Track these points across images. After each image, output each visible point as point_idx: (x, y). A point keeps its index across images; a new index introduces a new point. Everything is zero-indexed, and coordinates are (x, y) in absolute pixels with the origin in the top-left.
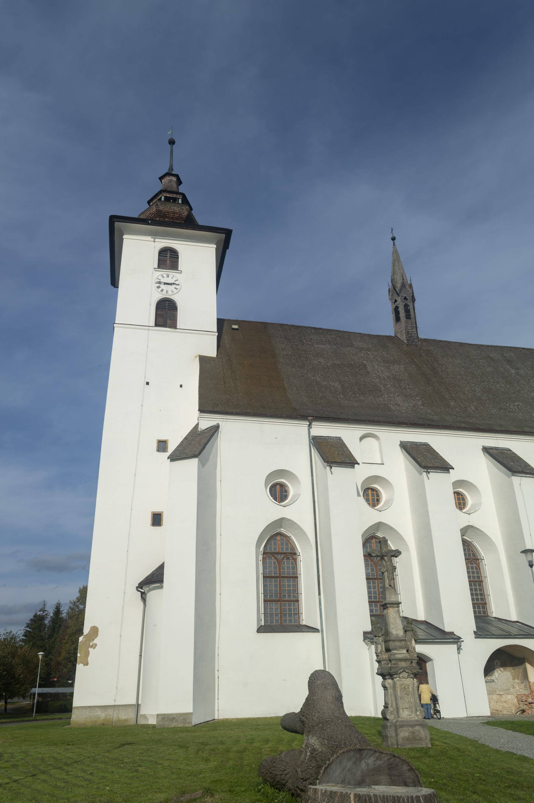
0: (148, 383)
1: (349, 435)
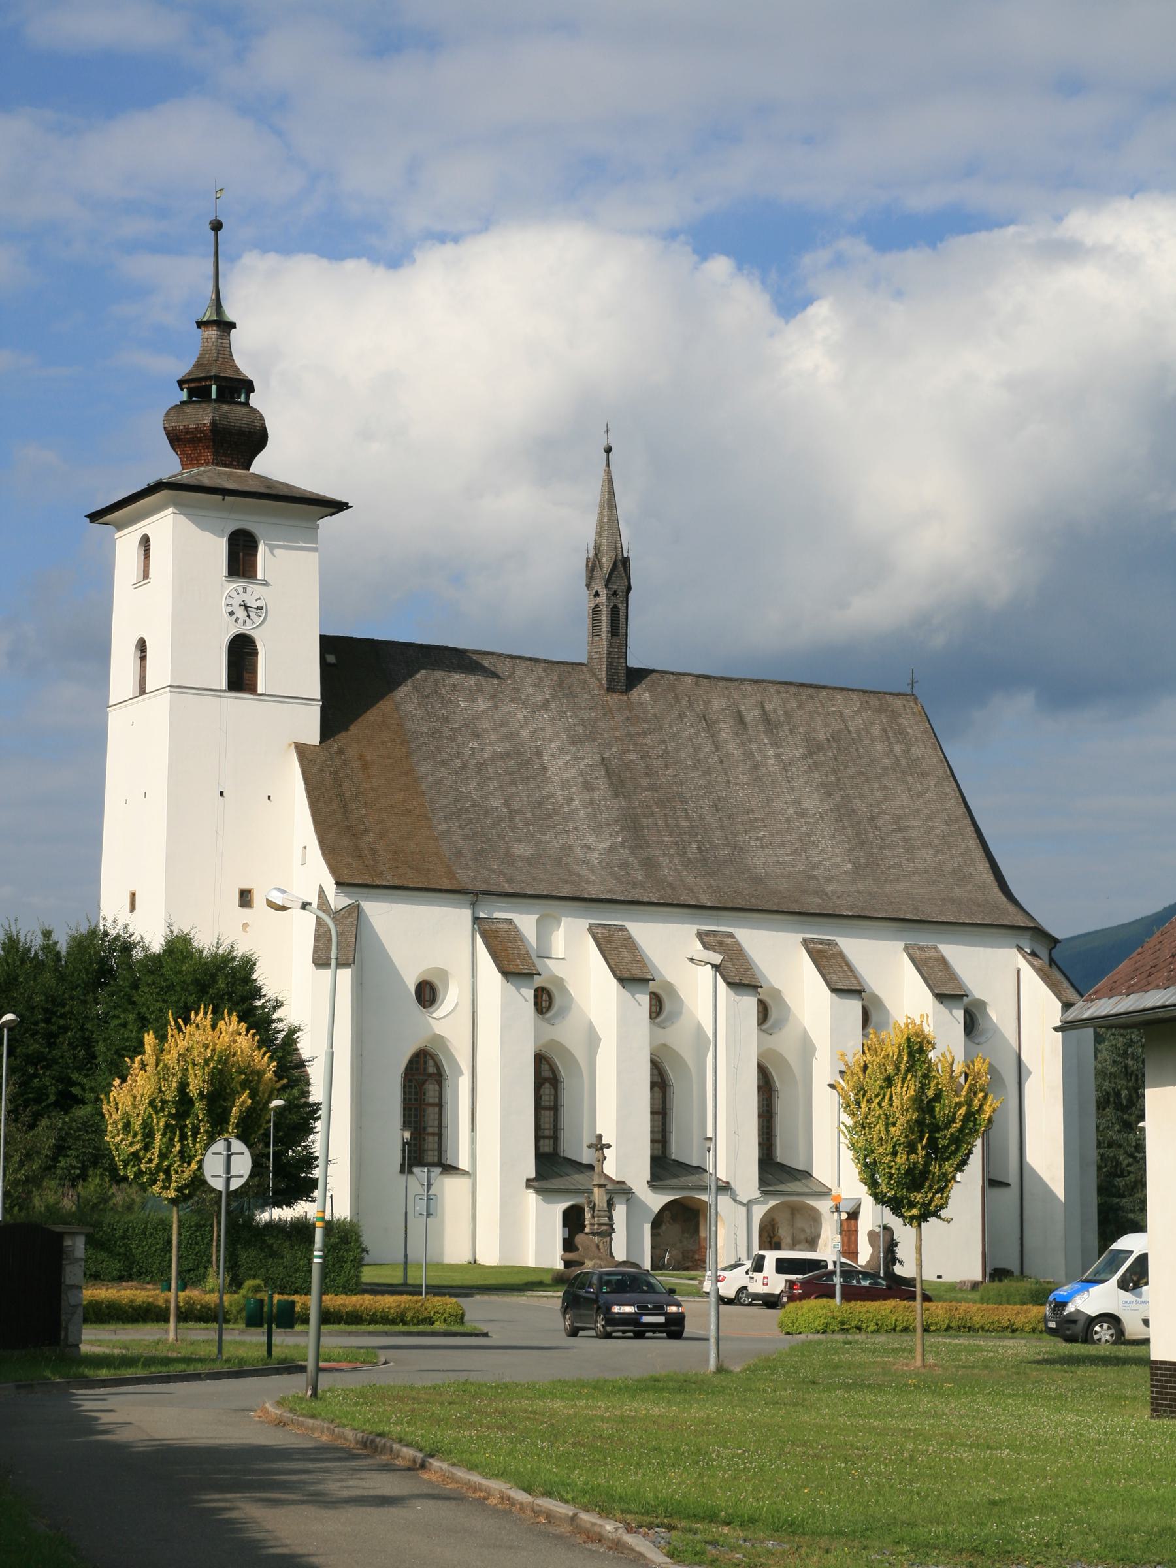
0: (222, 794)
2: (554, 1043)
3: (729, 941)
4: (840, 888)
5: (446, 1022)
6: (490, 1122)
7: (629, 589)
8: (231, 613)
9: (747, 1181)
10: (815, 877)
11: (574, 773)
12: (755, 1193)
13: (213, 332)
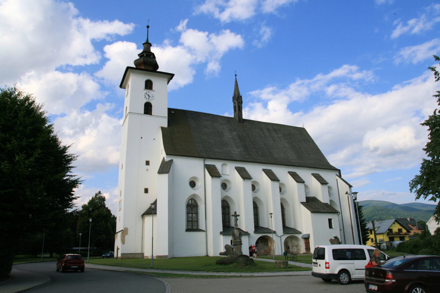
1: (218, 164)
2: (227, 197)
5: (198, 191)
6: (211, 217)
9: (280, 230)
12: (282, 234)
13: (146, 45)
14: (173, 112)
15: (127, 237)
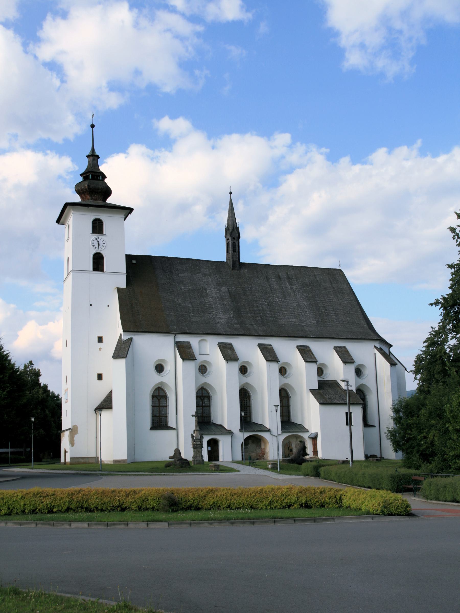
0: (91, 305)
1: (194, 341)
3: (269, 347)
4: (311, 329)
5: (167, 378)
7: (239, 237)
8: (93, 246)
10: (303, 326)
11: (218, 295)
12: (280, 432)
13: (91, 159)
14: (134, 262)
15: (76, 437)
